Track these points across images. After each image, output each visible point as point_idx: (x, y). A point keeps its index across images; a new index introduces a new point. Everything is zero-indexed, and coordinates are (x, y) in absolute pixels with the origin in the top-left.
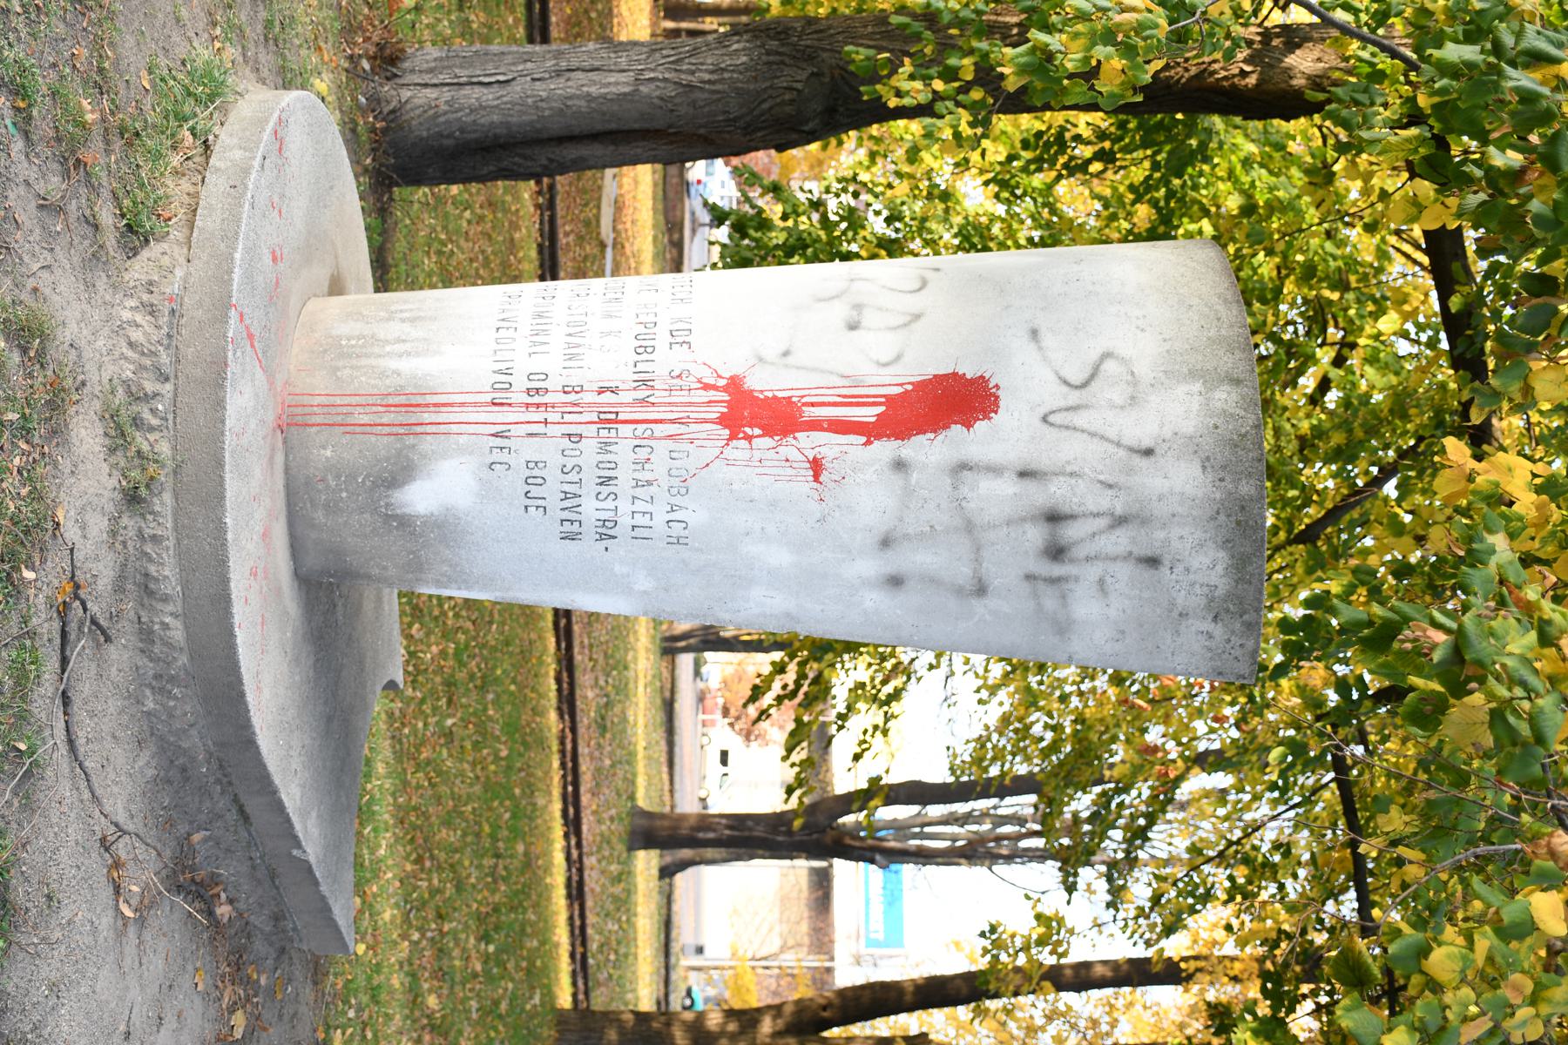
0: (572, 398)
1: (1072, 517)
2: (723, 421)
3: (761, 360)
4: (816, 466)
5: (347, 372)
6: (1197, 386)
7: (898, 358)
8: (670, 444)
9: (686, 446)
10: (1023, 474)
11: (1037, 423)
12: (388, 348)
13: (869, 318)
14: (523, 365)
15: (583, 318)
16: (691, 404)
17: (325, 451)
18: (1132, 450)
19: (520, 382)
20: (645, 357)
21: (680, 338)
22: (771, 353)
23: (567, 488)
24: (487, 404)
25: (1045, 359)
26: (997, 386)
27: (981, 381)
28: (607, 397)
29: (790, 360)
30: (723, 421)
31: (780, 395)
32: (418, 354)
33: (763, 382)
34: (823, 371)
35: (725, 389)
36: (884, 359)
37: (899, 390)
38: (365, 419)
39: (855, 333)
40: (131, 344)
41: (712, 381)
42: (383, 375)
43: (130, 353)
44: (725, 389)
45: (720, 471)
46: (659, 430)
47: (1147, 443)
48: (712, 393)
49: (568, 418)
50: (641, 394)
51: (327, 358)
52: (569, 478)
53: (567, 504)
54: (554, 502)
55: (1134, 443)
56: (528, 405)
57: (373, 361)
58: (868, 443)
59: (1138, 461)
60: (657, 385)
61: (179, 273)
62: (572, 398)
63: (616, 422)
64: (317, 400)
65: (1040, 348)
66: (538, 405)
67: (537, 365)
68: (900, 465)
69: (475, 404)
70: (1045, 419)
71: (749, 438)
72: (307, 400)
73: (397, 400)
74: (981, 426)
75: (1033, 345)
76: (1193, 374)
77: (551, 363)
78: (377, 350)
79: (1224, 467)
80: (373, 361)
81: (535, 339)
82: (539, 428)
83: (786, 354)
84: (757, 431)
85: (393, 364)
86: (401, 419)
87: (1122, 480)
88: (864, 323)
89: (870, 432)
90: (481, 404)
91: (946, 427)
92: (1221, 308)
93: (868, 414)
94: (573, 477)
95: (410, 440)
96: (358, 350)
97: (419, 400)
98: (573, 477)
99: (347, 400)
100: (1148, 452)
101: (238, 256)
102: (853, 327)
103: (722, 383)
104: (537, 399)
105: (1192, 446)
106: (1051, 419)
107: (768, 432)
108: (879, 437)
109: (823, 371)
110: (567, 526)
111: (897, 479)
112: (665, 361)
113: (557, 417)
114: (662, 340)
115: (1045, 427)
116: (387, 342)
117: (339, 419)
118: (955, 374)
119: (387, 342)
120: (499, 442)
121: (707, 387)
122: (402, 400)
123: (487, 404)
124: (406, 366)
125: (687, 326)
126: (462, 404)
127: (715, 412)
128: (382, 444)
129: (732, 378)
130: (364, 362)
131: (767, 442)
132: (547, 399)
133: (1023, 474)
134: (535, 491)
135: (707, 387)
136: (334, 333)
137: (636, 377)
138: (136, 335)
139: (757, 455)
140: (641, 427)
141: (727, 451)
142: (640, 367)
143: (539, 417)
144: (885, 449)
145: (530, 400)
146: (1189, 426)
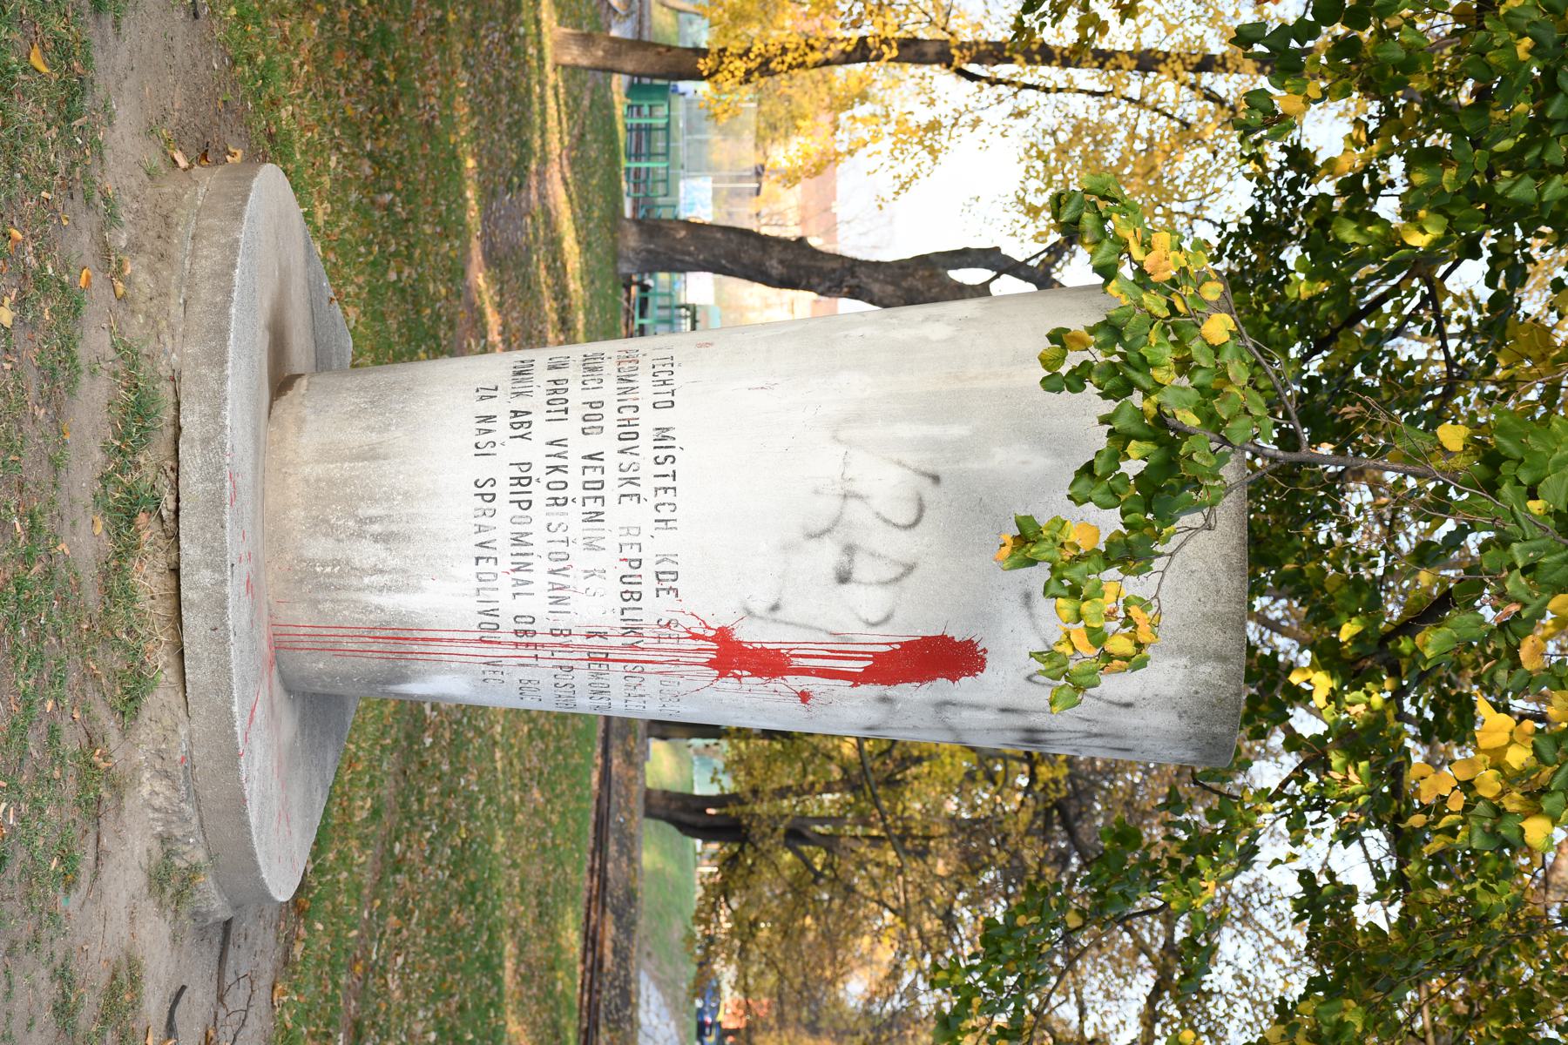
0: (561, 639)
1: (1050, 731)
2: (711, 664)
3: (749, 613)
4: (804, 697)
5: (328, 605)
6: (1184, 661)
7: (887, 619)
8: (661, 677)
9: (677, 679)
10: (1004, 710)
11: (1021, 680)
12: (366, 580)
13: (864, 569)
14: (509, 607)
15: (562, 547)
16: (679, 650)
17: (319, 664)
18: (1111, 702)
19: (507, 624)
20: (632, 604)
21: (667, 581)
22: (759, 607)
24: (476, 641)
25: (1035, 627)
26: (985, 651)
27: (969, 646)
28: (595, 641)
29: (779, 615)
30: (711, 664)
31: (769, 646)
32: (399, 590)
33: (750, 634)
34: (811, 628)
35: (713, 639)
36: (873, 619)
37: (888, 648)
38: (355, 647)
39: (845, 587)
40: (156, 810)
41: (701, 632)
42: (366, 609)
43: (156, 815)
44: (713, 639)
45: (709, 694)
46: (648, 667)
47: (1126, 699)
48: (701, 642)
49: (557, 655)
50: (629, 640)
51: (305, 589)
55: (1116, 699)
56: (516, 644)
57: (355, 596)
58: (855, 685)
59: (1116, 709)
60: (646, 632)
61: (183, 731)
62: (561, 639)
63: (606, 659)
64: (303, 631)
65: (1031, 616)
66: (527, 645)
67: (523, 606)
68: (884, 700)
69: (464, 641)
70: (1029, 678)
71: (739, 677)
72: (292, 630)
73: (384, 633)
74: (966, 681)
75: (1024, 612)
76: (1180, 650)
77: (536, 605)
78: (355, 582)
79: (1200, 718)
80: (355, 596)
81: (518, 575)
82: (533, 661)
83: (775, 608)
84: (745, 673)
85: (375, 599)
86: (389, 648)
87: (1100, 718)
88: (855, 576)
89: (855, 679)
90: (470, 641)
91: (933, 679)
92: (1224, 579)
93: (857, 666)
95: (403, 662)
96: (335, 581)
97: (407, 635)
99: (334, 631)
100: (1128, 705)
101: (235, 709)
102: (844, 578)
103: (711, 633)
104: (525, 639)
105: (1171, 703)
106: (1036, 678)
107: (756, 673)
108: (865, 682)
109: (811, 628)
111: (884, 707)
112: (654, 608)
113: (548, 654)
114: (648, 585)
115: (1030, 685)
116: (364, 572)
117: (328, 646)
118: (943, 637)
119: (364, 572)
121: (695, 637)
122: (390, 633)
123: (476, 641)
124: (389, 601)
125: (673, 568)
126: (451, 640)
127: (705, 657)
128: (375, 664)
129: (720, 629)
130: (343, 595)
131: (756, 680)
132: (536, 639)
133: (1004, 710)
135: (695, 637)
136: (309, 554)
137: (624, 624)
138: (158, 802)
139: (746, 687)
140: (630, 666)
141: (716, 684)
142: (628, 615)
143: (527, 653)
144: (871, 691)
145: (518, 640)
146: (1170, 691)
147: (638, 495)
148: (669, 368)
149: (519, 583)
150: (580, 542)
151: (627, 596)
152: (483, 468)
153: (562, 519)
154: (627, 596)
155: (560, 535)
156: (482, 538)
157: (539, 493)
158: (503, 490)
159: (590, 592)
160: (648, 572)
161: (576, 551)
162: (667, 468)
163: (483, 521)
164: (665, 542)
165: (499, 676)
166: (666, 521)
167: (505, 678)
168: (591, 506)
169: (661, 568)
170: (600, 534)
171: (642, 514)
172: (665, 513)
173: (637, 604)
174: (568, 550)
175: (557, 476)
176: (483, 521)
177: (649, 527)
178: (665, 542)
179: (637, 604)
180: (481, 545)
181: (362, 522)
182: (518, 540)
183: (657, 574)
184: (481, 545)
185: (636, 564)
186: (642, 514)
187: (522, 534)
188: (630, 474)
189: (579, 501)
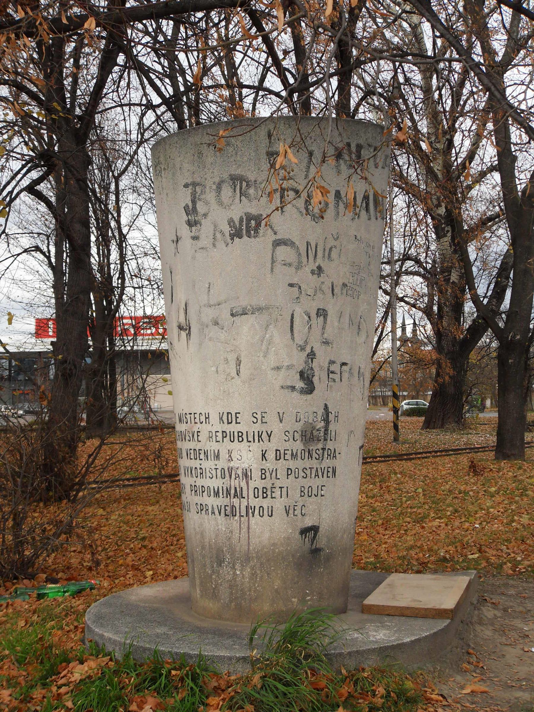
12: (238, 573)
20: (244, 437)
23: (313, 475)
52: (309, 475)
53: (320, 474)
54: (319, 482)
94: (308, 472)
98: (308, 472)
110: (330, 474)
114: (234, 428)
120: (291, 512)
125: (225, 414)
134: (315, 492)
142: (251, 439)
147: (198, 432)
148: (197, 416)
149: (235, 495)
150: (216, 462)
151: (240, 439)
152: (193, 509)
153: (207, 471)
154: (240, 439)
155: (214, 472)
156: (217, 512)
157: (200, 482)
158: (198, 499)
159: (240, 458)
160: (228, 428)
161: (222, 464)
162: (188, 416)
163: (210, 510)
164: (214, 418)
165: (298, 509)
166: (206, 418)
167: (300, 504)
168: (202, 456)
169: (225, 421)
170: (212, 452)
171: (205, 429)
172: (203, 418)
173: (245, 434)
174: (220, 469)
175: (193, 472)
176: (210, 510)
177: (209, 427)
178: (214, 418)
179: (245, 434)
180: (220, 513)
181: (213, 572)
182: (217, 494)
183: (228, 423)
184: (220, 513)
185: (224, 434)
186: (205, 429)
187: (214, 491)
188: (191, 435)
189: (201, 462)
